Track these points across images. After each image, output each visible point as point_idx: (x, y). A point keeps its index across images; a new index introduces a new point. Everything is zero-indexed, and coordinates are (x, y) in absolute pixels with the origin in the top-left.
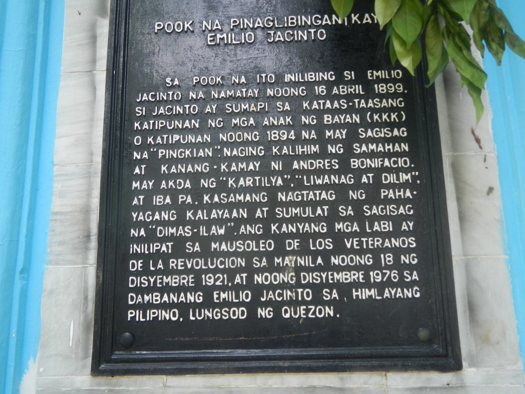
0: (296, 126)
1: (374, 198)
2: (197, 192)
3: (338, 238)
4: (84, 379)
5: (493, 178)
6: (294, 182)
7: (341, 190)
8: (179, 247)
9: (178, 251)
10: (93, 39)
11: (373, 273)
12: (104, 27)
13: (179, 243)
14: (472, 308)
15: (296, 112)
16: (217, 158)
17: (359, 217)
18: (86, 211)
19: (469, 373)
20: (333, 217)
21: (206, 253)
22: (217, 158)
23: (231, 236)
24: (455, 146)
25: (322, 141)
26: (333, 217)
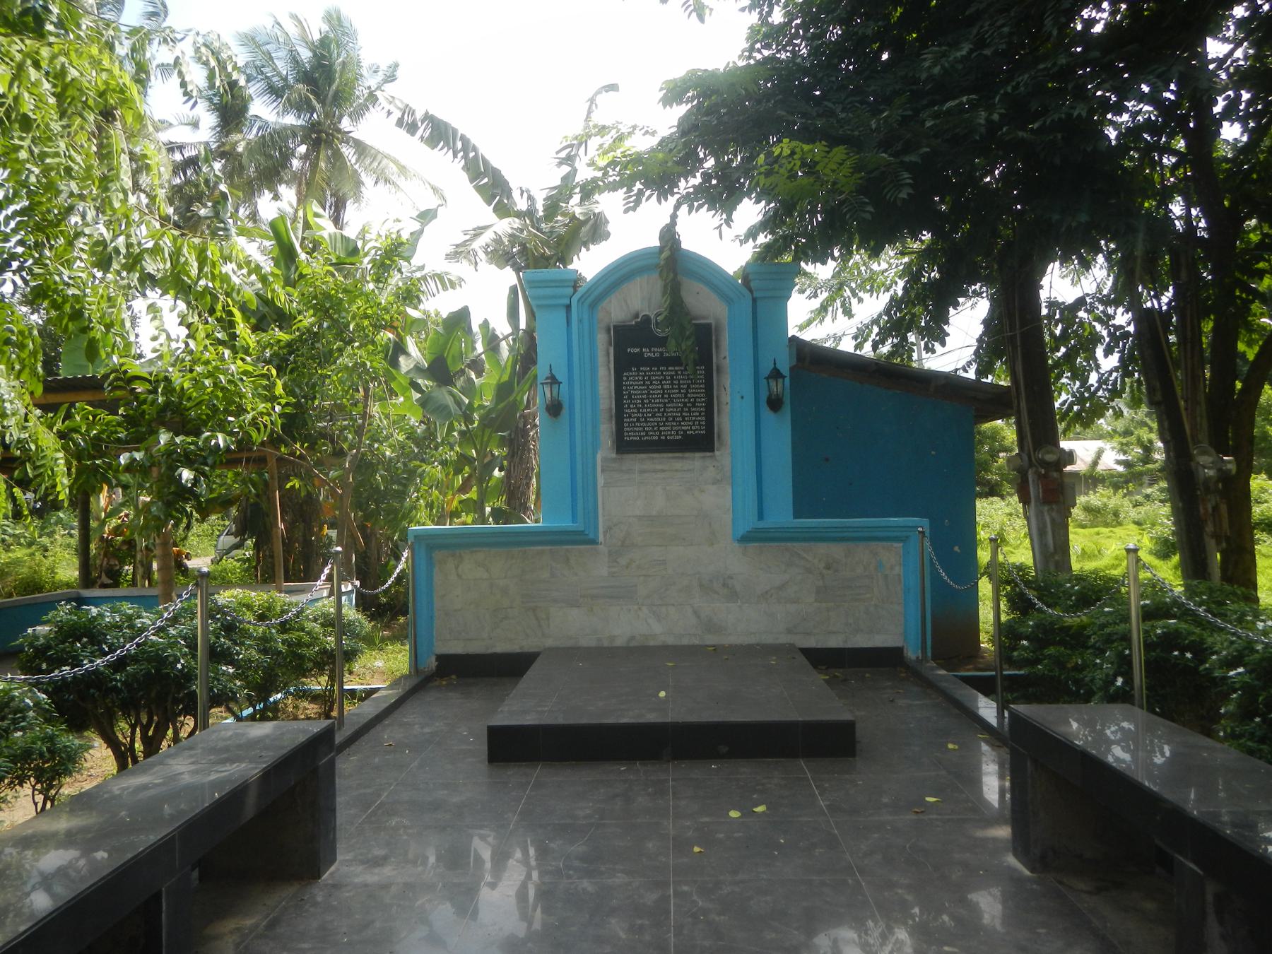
0: (672, 384)
1: (694, 406)
2: (643, 404)
3: (683, 417)
4: (614, 455)
5: (728, 399)
6: (671, 401)
7: (685, 403)
8: (638, 420)
9: (638, 420)
10: (608, 354)
11: (691, 427)
12: (612, 350)
13: (638, 419)
14: (719, 436)
15: (672, 379)
16: (648, 394)
17: (689, 411)
18: (610, 409)
19: (717, 453)
20: (682, 411)
21: (646, 421)
22: (648, 394)
23: (653, 416)
24: (718, 390)
25: (680, 389)
26: (682, 411)
